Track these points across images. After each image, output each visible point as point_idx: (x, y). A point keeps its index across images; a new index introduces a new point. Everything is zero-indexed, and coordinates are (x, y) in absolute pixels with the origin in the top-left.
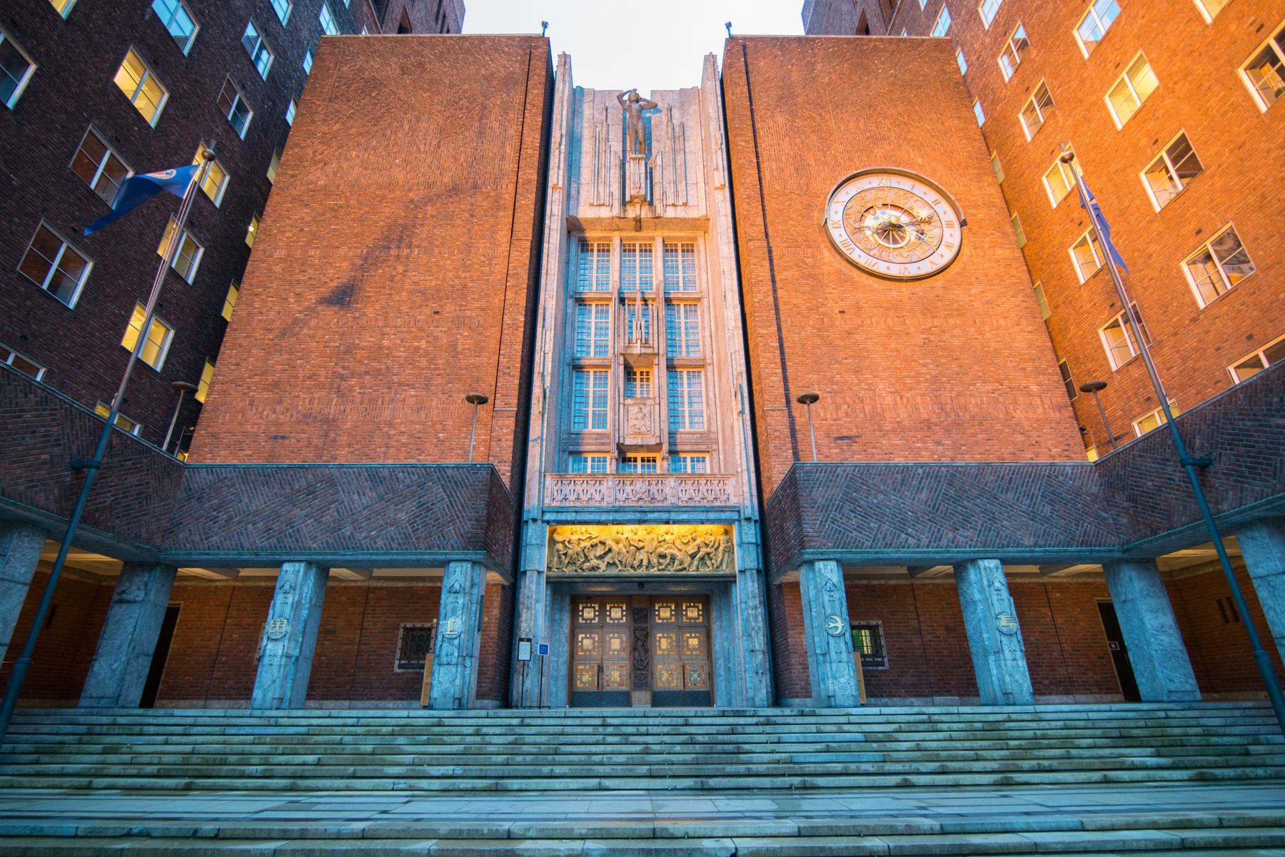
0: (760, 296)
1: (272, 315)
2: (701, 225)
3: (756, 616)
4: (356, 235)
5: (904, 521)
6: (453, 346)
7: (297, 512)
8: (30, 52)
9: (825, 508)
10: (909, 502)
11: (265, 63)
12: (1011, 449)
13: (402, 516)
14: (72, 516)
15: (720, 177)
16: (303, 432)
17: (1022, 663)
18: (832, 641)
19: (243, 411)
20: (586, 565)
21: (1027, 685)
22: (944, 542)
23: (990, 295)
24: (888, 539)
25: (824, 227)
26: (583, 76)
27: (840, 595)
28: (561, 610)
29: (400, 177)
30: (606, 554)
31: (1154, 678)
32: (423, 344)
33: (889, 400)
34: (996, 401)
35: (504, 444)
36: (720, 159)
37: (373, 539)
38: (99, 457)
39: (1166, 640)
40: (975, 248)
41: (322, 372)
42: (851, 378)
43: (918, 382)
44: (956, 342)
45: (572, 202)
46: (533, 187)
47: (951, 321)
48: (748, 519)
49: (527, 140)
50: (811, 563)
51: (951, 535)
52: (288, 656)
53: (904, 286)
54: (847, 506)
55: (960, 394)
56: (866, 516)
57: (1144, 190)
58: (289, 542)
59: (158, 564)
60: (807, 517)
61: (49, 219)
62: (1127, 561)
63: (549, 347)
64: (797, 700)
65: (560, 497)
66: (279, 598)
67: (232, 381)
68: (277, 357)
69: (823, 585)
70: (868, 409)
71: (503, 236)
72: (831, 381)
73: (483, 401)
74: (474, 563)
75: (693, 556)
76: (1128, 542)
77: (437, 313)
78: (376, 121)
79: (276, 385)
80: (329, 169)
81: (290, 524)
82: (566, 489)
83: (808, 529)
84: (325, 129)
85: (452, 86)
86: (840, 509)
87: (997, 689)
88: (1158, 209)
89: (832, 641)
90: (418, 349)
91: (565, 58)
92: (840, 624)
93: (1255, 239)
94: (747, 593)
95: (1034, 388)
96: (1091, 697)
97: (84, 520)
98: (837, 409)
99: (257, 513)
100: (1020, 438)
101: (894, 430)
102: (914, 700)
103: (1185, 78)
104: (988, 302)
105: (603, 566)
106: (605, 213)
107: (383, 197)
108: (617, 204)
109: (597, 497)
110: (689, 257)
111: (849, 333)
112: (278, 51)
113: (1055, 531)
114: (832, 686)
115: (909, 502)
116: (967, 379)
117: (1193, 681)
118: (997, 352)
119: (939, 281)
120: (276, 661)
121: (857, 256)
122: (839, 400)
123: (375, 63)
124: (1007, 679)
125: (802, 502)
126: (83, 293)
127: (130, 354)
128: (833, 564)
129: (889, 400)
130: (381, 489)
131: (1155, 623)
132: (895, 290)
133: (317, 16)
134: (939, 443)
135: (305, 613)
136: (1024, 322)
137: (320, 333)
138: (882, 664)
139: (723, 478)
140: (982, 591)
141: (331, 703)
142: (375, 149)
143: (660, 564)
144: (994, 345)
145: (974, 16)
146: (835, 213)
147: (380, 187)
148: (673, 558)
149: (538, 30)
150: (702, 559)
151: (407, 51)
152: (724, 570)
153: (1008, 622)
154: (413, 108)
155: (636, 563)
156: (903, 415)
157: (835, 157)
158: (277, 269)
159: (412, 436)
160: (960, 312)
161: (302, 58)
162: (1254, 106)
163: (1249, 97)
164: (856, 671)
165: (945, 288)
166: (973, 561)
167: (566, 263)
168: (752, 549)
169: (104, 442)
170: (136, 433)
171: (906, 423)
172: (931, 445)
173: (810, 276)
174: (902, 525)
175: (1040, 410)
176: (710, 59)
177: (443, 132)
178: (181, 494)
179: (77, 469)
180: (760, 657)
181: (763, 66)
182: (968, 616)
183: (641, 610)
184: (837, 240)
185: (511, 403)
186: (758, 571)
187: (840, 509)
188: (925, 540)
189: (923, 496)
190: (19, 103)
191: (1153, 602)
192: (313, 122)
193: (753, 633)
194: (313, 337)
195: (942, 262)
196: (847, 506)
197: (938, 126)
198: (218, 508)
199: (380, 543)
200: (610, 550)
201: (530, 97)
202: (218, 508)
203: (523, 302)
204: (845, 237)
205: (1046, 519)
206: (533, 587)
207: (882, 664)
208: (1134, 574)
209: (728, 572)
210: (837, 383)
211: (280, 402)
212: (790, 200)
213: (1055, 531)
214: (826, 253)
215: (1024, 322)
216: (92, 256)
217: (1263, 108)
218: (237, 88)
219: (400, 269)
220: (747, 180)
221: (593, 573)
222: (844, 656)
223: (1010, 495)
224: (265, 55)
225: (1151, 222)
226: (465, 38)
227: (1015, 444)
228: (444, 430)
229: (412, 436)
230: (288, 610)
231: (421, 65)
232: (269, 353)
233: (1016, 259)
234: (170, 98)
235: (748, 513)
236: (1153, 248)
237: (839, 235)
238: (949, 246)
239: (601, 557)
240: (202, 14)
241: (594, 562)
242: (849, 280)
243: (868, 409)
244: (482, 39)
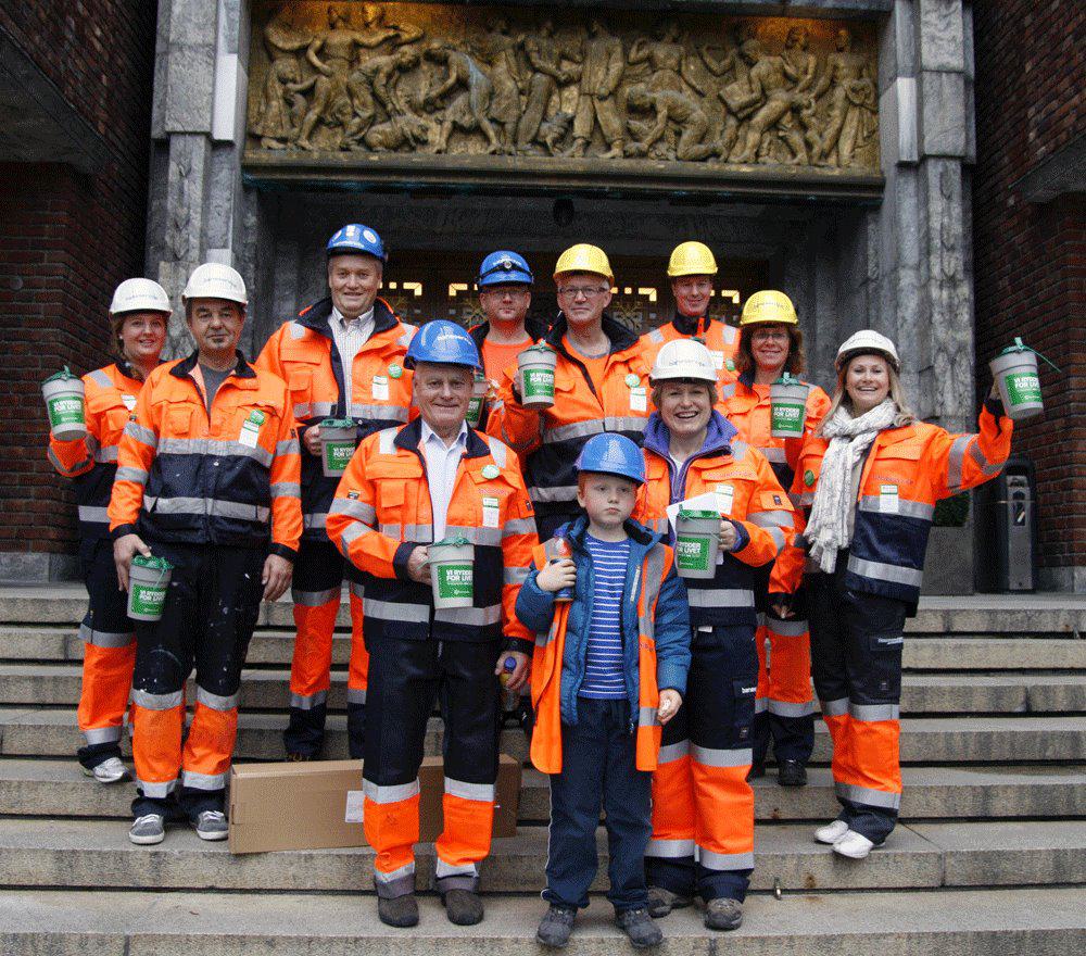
3: (951, 309)
20: (377, 133)
30: (447, 95)
75: (744, 116)
105: (437, 135)
143: (632, 135)
148: (677, 120)
150: (773, 125)
152: (846, 163)
155: (550, 132)
193: (940, 363)
200: (462, 84)
206: (194, 190)
209: (858, 169)
221: (402, 158)
239: (431, 106)
241: (409, 122)
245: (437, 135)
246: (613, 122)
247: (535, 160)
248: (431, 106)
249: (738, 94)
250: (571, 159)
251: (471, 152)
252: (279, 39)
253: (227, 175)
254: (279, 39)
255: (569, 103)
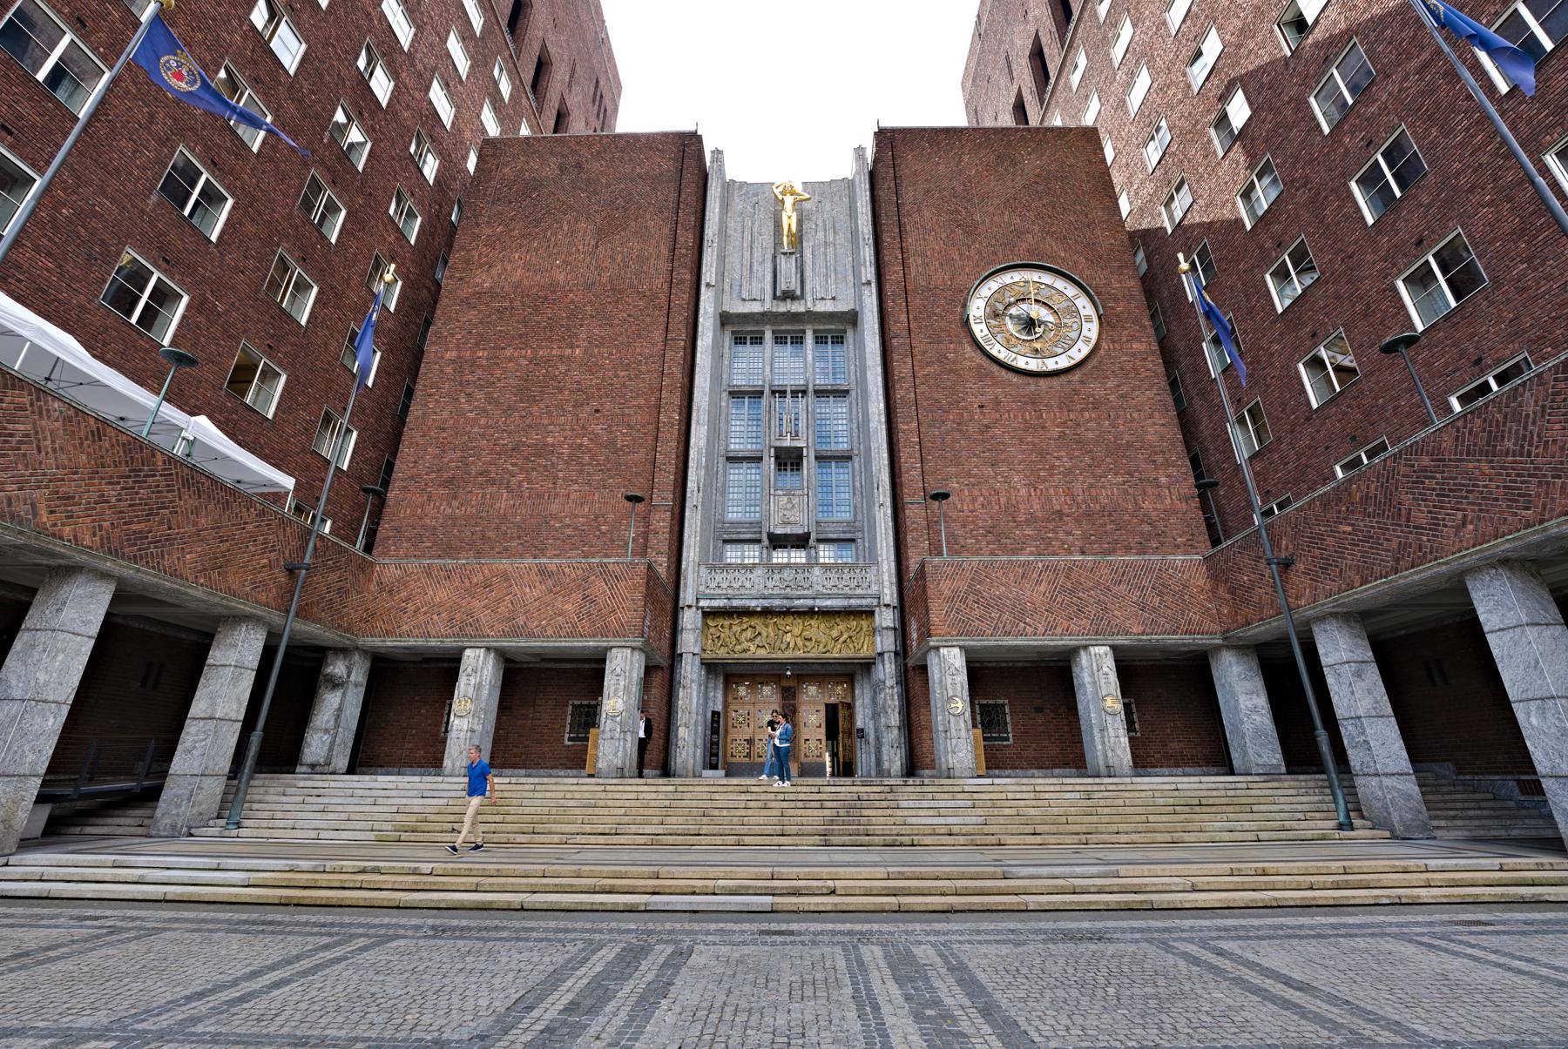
0: (902, 393)
1: (445, 414)
2: (852, 318)
4: (520, 336)
5: (1023, 612)
6: (612, 443)
7: (475, 603)
8: (227, 188)
9: (951, 599)
10: (1028, 593)
11: (430, 168)
12: (1138, 539)
13: (568, 607)
14: (288, 612)
15: (869, 273)
16: (476, 525)
17: (1125, 740)
18: (952, 719)
19: (422, 506)
20: (738, 648)
21: (1127, 758)
22: (1059, 630)
23: (1125, 389)
24: (1008, 628)
25: (966, 323)
26: (736, 170)
27: (962, 678)
28: (715, 688)
29: (561, 277)
31: (1245, 753)
32: (586, 441)
33: (1023, 492)
34: (1126, 492)
35: (661, 537)
36: (868, 253)
37: (544, 628)
38: (307, 560)
39: (1258, 719)
40: (1113, 342)
41: (492, 468)
42: (989, 471)
43: (1052, 475)
44: (1091, 435)
45: (726, 297)
46: (687, 286)
47: (1086, 414)
48: (887, 606)
49: (681, 239)
50: (937, 648)
51: (1065, 624)
52: (473, 731)
53: (1042, 382)
54: (972, 597)
55: (1091, 486)
56: (988, 606)
57: (1268, 291)
58: (469, 630)
59: (357, 648)
60: (934, 606)
61: (248, 339)
62: (1227, 647)
63: (703, 443)
64: (927, 772)
65: (713, 585)
66: (462, 679)
67: (412, 478)
68: (452, 455)
69: (949, 669)
70: (1003, 500)
71: (658, 335)
72: (969, 475)
73: (639, 499)
74: (633, 649)
76: (1228, 631)
77: (597, 411)
78: (538, 222)
79: (451, 480)
80: (494, 272)
81: (470, 615)
82: (719, 578)
83: (935, 618)
84: (488, 231)
85: (608, 185)
86: (964, 600)
87: (1101, 763)
88: (1280, 310)
89: (952, 719)
90: (581, 445)
91: (717, 153)
92: (960, 705)
93: (1361, 346)
94: (887, 671)
95: (1163, 480)
96: (1198, 770)
97: (297, 615)
98: (974, 500)
99: (441, 604)
100: (1147, 528)
101: (1027, 521)
102: (1035, 771)
103: (1305, 185)
104: (1122, 396)
105: (753, 648)
106: (756, 308)
107: (546, 298)
108: (768, 296)
109: (748, 585)
110: (838, 348)
111: (987, 427)
112: (442, 154)
113: (1162, 620)
114: (952, 761)
115: (1028, 593)
116: (1099, 471)
117: (1279, 756)
118: (1129, 445)
119: (1076, 376)
120: (462, 735)
121: (998, 351)
122: (976, 493)
123: (535, 164)
124: (1110, 754)
125: (930, 593)
126: (279, 403)
127: (328, 462)
128: (957, 650)
129: (1023, 492)
130: (550, 582)
131: (1249, 704)
132: (1033, 385)
133: (479, 116)
134: (1069, 533)
135: (485, 692)
136: (1157, 415)
137: (490, 431)
138: (1007, 739)
139: (864, 568)
140: (1092, 675)
141: (510, 772)
142: (536, 250)
144: (1126, 437)
145: (1122, 104)
146: (977, 308)
147: (542, 288)
149: (692, 128)
151: (566, 151)
153: (1114, 703)
154: (571, 207)
156: (1037, 507)
157: (979, 252)
158: (449, 370)
159: (576, 529)
160: (1096, 405)
161: (465, 158)
162: (1363, 218)
163: (1358, 210)
164: (976, 748)
165: (1081, 382)
166: (1086, 647)
167: (718, 356)
168: (891, 634)
169: (311, 545)
170: (327, 530)
171: (1039, 514)
172: (1061, 535)
173: (951, 371)
174: (1020, 615)
175: (1168, 501)
176: (859, 151)
177: (602, 234)
178: (373, 587)
179: (291, 571)
180: (896, 732)
181: (910, 163)
182: (1079, 697)
183: (789, 688)
184: (978, 335)
185: (664, 497)
186: (896, 654)
187: (964, 600)
188: (1041, 629)
189: (1042, 588)
190: (220, 237)
191: (1248, 685)
192: (478, 225)
194: (483, 435)
195: (1079, 357)
196: (972, 597)
197: (1082, 217)
198: (406, 601)
199: (550, 632)
201: (683, 196)
202: (406, 601)
203: (677, 402)
204: (986, 331)
205: (1154, 610)
207: (1007, 739)
208: (1233, 660)
209: (868, 654)
210: (975, 476)
211: (455, 498)
212: (934, 295)
213: (1162, 620)
214: (968, 348)
215: (1157, 415)
216: (285, 369)
217: (1370, 221)
218: (408, 195)
219: (563, 368)
220: (894, 274)
221: (744, 655)
222: (963, 733)
223: (1123, 587)
224: (430, 158)
225: (1274, 322)
226: (620, 136)
227: (1142, 534)
228: (605, 523)
229: (576, 529)
230: (471, 690)
231: (579, 166)
232: (444, 451)
233: (1153, 352)
234: (348, 214)
235: (887, 600)
236: (1275, 347)
237: (980, 330)
238: (1087, 341)
239: (751, 640)
240: (373, 129)
241: (745, 645)
242: (989, 375)
243: (1003, 500)
244: (634, 139)
245: (753, 648)
246: (800, 644)
247: (780, 655)
248: (751, 640)
249: (835, 633)
250: (789, 654)
251: (762, 653)
252: (710, 623)
253: (697, 662)
254: (710, 623)
255: (788, 637)
